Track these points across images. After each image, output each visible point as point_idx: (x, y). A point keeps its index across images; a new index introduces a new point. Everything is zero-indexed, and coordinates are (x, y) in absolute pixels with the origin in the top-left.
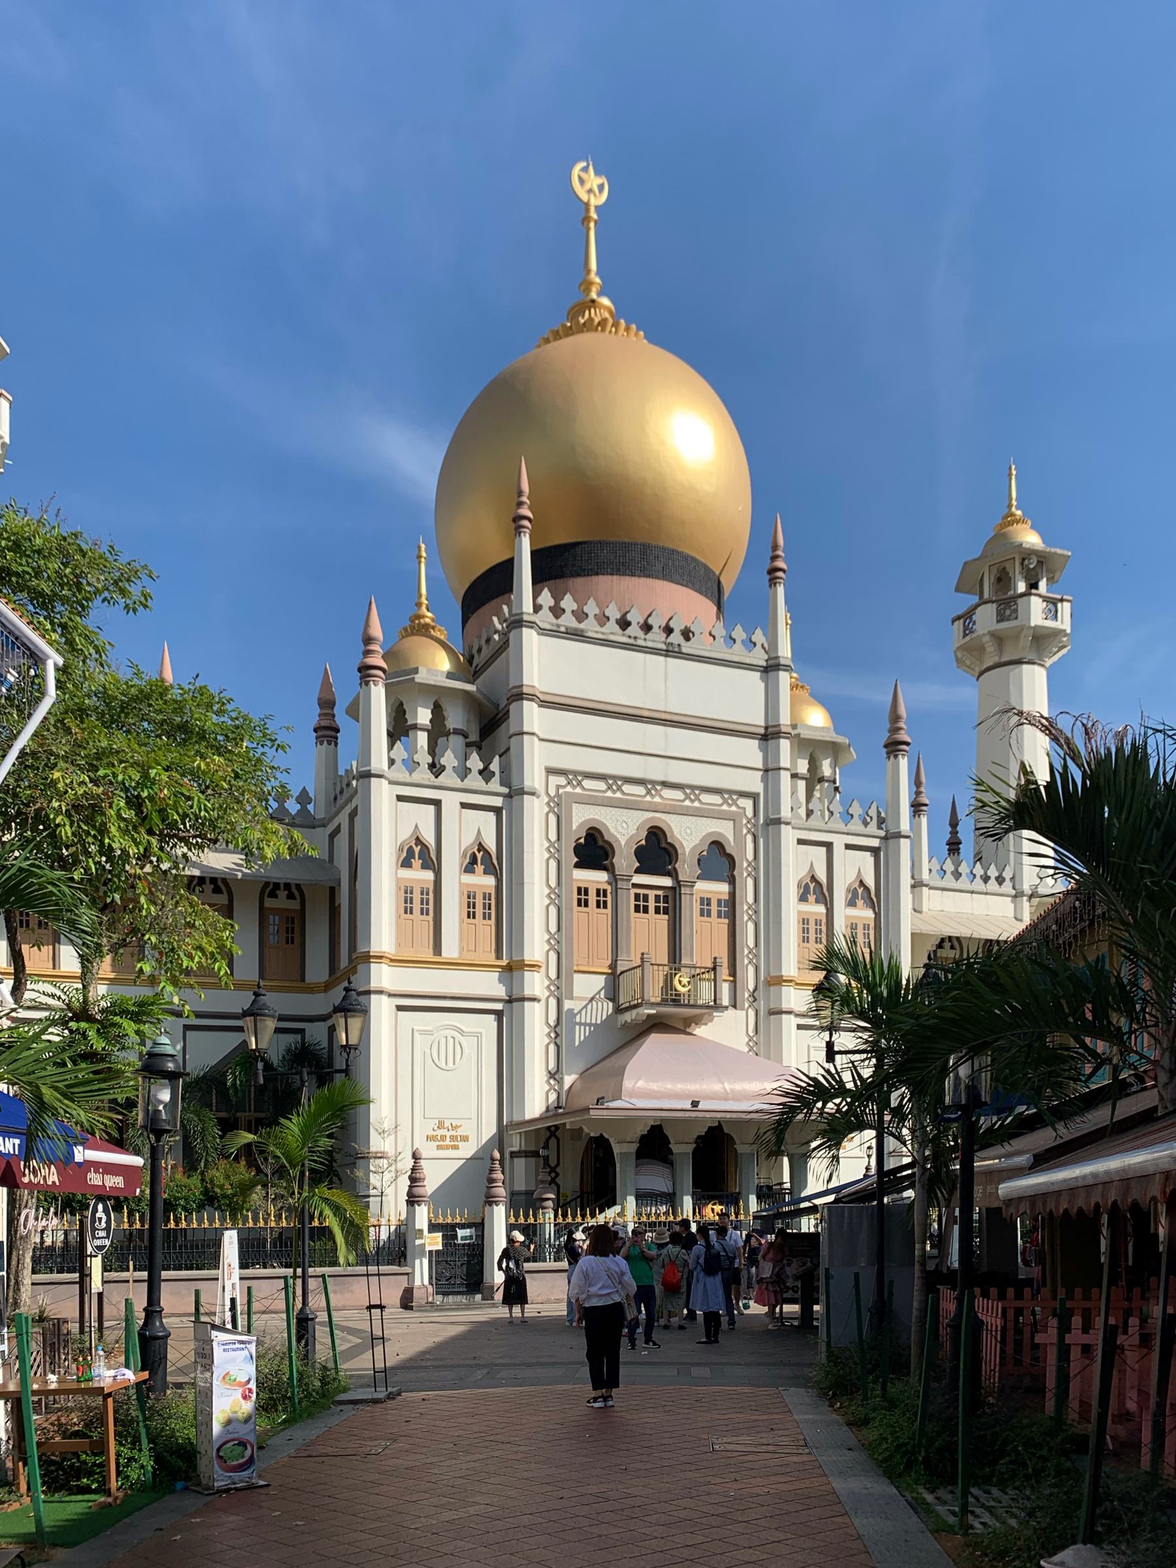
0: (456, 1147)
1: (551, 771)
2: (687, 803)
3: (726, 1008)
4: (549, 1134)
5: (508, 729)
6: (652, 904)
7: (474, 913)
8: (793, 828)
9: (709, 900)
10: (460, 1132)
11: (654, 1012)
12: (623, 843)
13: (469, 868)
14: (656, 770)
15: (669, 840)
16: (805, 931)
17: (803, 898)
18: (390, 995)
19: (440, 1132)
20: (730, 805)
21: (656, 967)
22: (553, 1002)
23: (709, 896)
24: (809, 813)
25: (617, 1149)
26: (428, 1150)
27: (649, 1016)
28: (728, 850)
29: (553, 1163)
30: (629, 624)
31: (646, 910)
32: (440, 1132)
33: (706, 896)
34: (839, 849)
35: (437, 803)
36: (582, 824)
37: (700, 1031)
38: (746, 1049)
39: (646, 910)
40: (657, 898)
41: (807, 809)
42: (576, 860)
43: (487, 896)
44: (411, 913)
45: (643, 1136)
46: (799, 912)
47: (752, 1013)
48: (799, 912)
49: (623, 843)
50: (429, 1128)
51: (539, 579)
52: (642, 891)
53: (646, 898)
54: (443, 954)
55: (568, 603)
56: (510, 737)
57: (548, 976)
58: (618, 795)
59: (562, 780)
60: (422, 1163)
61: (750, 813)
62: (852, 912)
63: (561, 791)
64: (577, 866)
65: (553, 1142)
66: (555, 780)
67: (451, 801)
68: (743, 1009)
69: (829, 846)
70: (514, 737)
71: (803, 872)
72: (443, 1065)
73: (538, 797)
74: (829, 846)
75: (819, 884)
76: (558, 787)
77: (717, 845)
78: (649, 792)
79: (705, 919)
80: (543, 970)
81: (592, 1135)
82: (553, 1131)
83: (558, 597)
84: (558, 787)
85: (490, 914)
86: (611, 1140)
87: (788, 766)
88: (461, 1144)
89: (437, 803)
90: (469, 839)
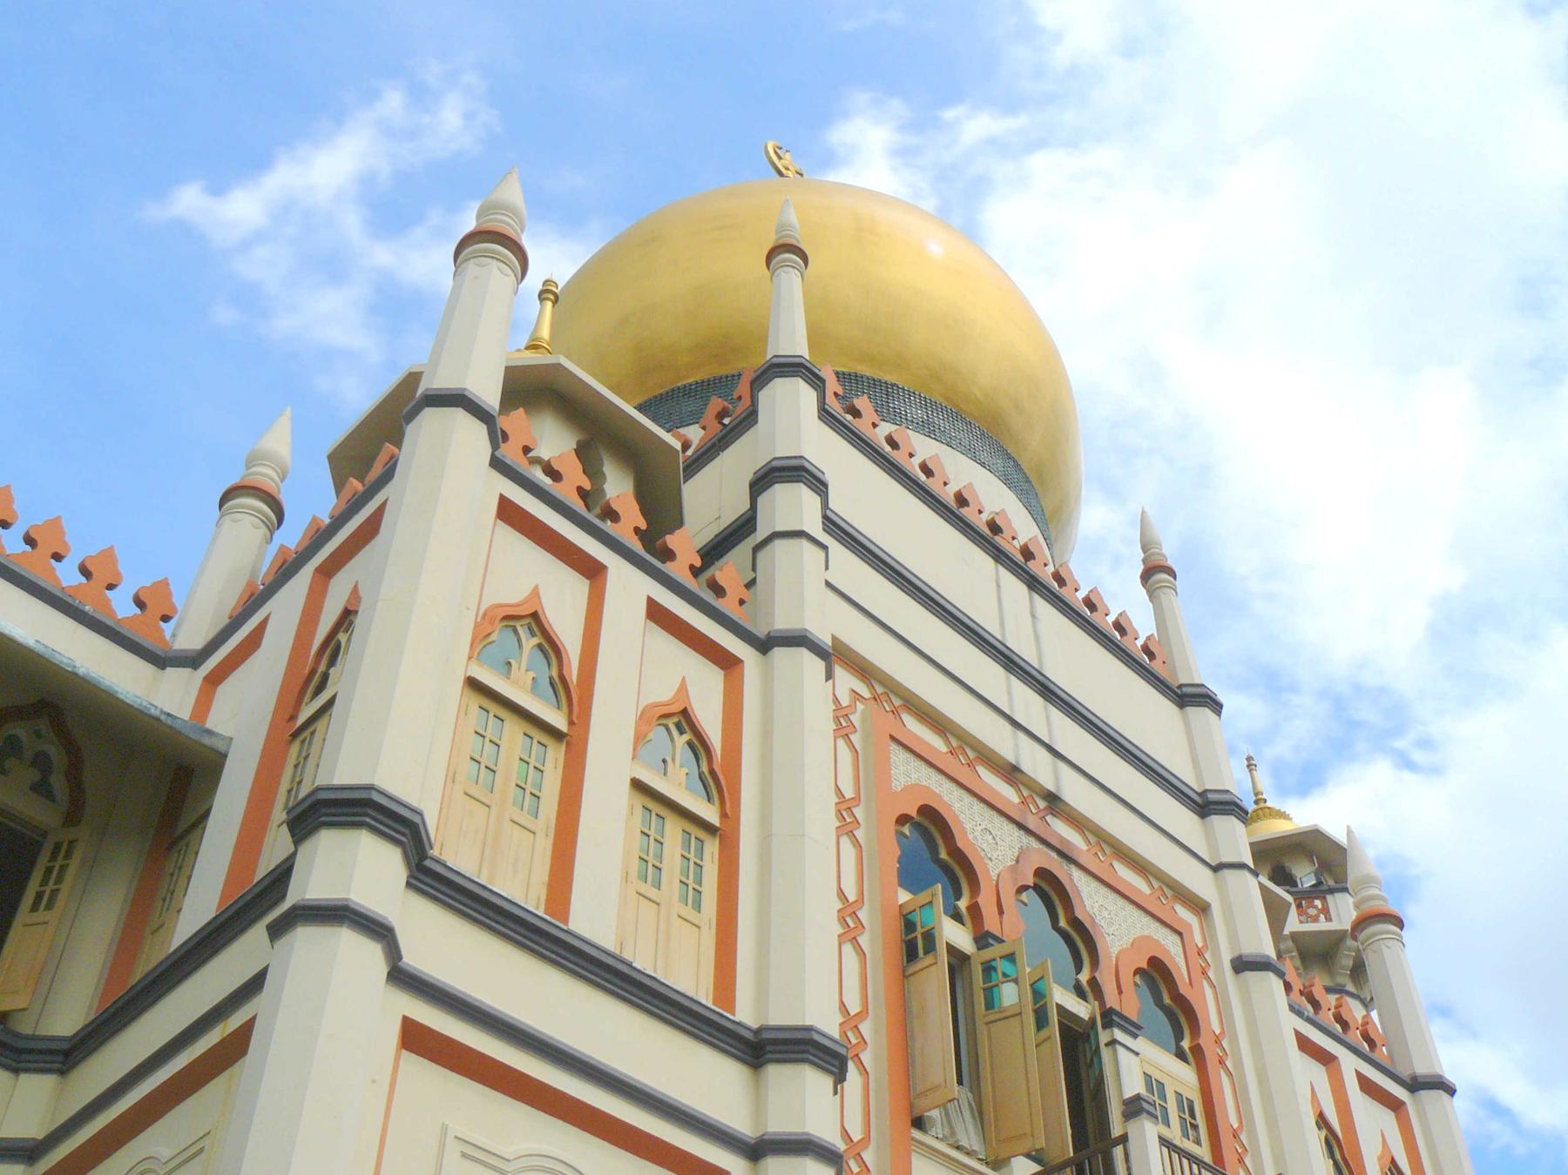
12: (994, 875)
15: (1079, 914)
33: (1156, 1075)
36: (905, 789)
42: (898, 865)
49: (994, 875)
56: (757, 549)
63: (860, 706)
66: (846, 681)
77: (1156, 973)
78: (1024, 802)
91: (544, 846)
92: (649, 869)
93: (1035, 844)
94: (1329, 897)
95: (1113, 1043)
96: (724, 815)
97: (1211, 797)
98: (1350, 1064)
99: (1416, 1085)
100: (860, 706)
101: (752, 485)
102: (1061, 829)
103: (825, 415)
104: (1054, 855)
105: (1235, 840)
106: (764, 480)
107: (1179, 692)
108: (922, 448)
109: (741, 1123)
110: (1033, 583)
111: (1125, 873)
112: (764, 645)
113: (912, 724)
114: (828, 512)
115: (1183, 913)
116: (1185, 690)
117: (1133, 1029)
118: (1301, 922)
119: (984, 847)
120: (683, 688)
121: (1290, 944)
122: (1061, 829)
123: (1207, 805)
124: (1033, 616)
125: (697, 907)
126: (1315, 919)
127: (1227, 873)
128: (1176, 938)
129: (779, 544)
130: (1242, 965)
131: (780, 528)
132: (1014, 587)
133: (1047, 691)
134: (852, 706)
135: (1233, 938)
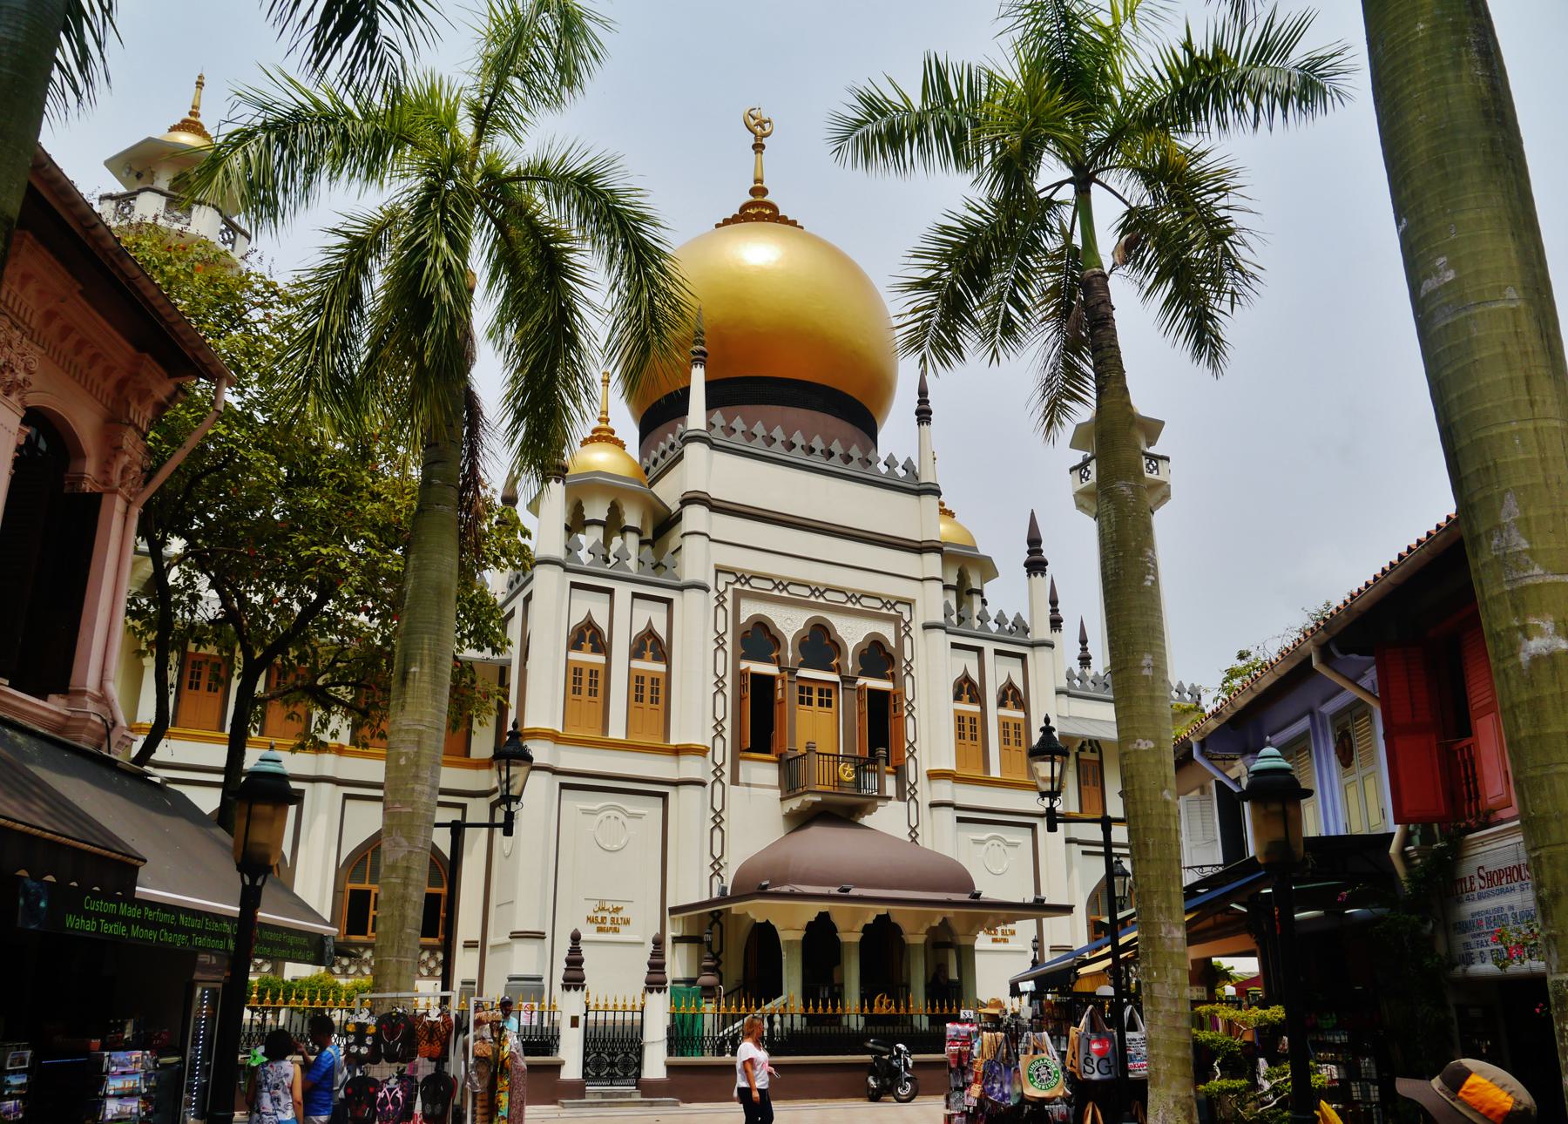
0: (616, 931)
3: (890, 798)
4: (711, 920)
5: (680, 528)
6: (815, 697)
8: (947, 633)
10: (621, 914)
11: (818, 799)
18: (556, 772)
19: (600, 915)
21: (821, 757)
22: (718, 787)
24: (961, 619)
25: (784, 936)
26: (588, 933)
27: (814, 803)
29: (716, 949)
30: (794, 446)
31: (810, 702)
32: (600, 915)
35: (610, 591)
37: (866, 820)
38: (910, 840)
39: (810, 702)
40: (821, 692)
41: (959, 616)
43: (655, 681)
45: (810, 923)
46: (955, 710)
47: (912, 804)
48: (955, 710)
50: (589, 909)
51: (712, 404)
52: (806, 684)
53: (810, 691)
54: (610, 736)
55: (738, 424)
56: (683, 536)
57: (714, 762)
58: (785, 594)
59: (732, 578)
60: (582, 946)
62: (1003, 712)
63: (730, 588)
64: (745, 657)
65: (716, 926)
66: (723, 578)
67: (623, 591)
68: (905, 801)
69: (979, 650)
70: (687, 538)
71: (959, 673)
72: (607, 846)
73: (706, 589)
74: (979, 650)
75: (972, 684)
80: (709, 754)
81: (758, 921)
82: (716, 917)
83: (729, 419)
85: (657, 698)
86: (778, 927)
87: (940, 576)
88: (622, 928)
89: (610, 591)
90: (639, 627)
91: (600, 706)
96: (667, 667)
97: (924, 544)
98: (989, 648)
99: (1033, 645)
100: (730, 588)
105: (932, 564)
107: (916, 487)
109: (675, 777)
112: (681, 589)
114: (714, 503)
115: (899, 607)
116: (922, 487)
119: (786, 626)
120: (650, 621)
123: (920, 548)
125: (657, 703)
127: (926, 583)
129: (687, 538)
130: (926, 627)
131: (688, 530)
134: (726, 590)
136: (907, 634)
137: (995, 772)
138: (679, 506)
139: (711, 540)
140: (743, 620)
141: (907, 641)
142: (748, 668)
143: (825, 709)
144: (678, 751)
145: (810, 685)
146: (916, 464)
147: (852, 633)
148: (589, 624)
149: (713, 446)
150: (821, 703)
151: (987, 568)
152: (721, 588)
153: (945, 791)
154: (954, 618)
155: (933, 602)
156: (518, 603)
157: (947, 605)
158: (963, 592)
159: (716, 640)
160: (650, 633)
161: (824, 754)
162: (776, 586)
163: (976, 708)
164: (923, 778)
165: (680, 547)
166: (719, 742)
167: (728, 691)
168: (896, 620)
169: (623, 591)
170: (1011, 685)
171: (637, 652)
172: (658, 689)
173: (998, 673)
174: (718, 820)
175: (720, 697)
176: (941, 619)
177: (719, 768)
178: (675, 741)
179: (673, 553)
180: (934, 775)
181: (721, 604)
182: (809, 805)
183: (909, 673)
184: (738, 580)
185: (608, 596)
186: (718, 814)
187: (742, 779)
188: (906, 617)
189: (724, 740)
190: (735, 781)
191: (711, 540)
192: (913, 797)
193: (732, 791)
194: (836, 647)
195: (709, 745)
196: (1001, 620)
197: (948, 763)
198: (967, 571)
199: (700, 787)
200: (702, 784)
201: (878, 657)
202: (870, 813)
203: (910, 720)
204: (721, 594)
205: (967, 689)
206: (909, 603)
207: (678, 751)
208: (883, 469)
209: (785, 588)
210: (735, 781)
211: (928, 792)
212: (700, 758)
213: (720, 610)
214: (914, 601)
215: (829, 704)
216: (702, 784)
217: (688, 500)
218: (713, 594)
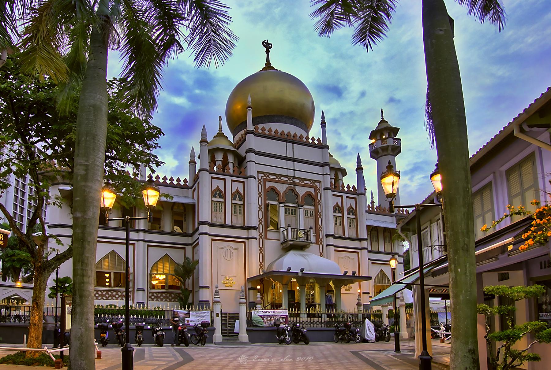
1: (259, 172)
2: (300, 183)
7: (236, 212)
9: (308, 211)
11: (292, 243)
13: (233, 198)
14: (291, 173)
15: (295, 193)
16: (336, 221)
17: (335, 212)
20: (313, 184)
22: (261, 240)
23: (307, 210)
28: (313, 197)
31: (289, 214)
34: (344, 198)
35: (224, 179)
40: (292, 210)
44: (216, 211)
49: (281, 193)
53: (289, 209)
58: (280, 180)
59: (263, 175)
61: (319, 187)
62: (349, 216)
66: (260, 175)
69: (341, 196)
73: (255, 178)
74: (341, 196)
76: (261, 177)
77: (309, 194)
78: (289, 180)
79: (307, 217)
80: (258, 229)
84: (261, 177)
87: (329, 173)
89: (224, 179)
90: (234, 190)
92: (235, 213)
93: (289, 185)
94: (387, 139)
95: (299, 209)
97: (324, 164)
98: (344, 195)
100: (262, 178)
101: (246, 152)
102: (296, 180)
103: (256, 135)
104: (293, 186)
105: (327, 169)
106: (247, 152)
108: (275, 127)
110: (293, 143)
111: (306, 182)
112: (247, 178)
113: (270, 176)
115: (316, 184)
116: (323, 146)
117: (302, 206)
118: (382, 144)
121: (380, 149)
122: (296, 180)
124: (293, 148)
126: (384, 144)
128: (313, 189)
129: (248, 162)
130: (325, 189)
132: (290, 145)
133: (294, 160)
135: (324, 185)
136: (319, 192)
137: (346, 235)
138: (245, 154)
139: (256, 163)
140: (267, 187)
141: (319, 194)
142: (269, 203)
143: (293, 215)
144: (248, 228)
145: (289, 208)
146: (321, 139)
147: (301, 191)
148: (218, 189)
149: (255, 135)
150: (292, 214)
151: (344, 172)
152: (260, 178)
153: (332, 241)
154: (334, 187)
155: (328, 181)
156: (196, 185)
157: (331, 182)
158: (337, 180)
159: (259, 194)
160: (237, 191)
161: (293, 228)
162: (277, 178)
163: (340, 215)
164: (325, 237)
165: (246, 167)
166: (261, 226)
167: (263, 210)
168: (315, 187)
169: (229, 179)
170: (351, 207)
171: (234, 197)
172: (241, 209)
173: (348, 203)
174: (261, 250)
175: (260, 212)
176: (329, 186)
177: (261, 234)
178: (246, 225)
179: (245, 169)
180: (328, 236)
181: (260, 183)
182: (289, 245)
183: (319, 204)
184: (265, 176)
185: (224, 181)
186: (261, 248)
187: (268, 238)
188: (319, 187)
189: (262, 225)
190: (266, 238)
191: (256, 163)
192: (321, 243)
193: (265, 240)
194: (297, 195)
195: (258, 227)
196: (348, 187)
197: (332, 232)
198: (337, 173)
199: (255, 240)
200: (256, 238)
201: (311, 199)
202: (308, 248)
203: (320, 219)
204: (260, 180)
205: (338, 209)
206: (320, 182)
207: (248, 228)
208: (311, 141)
209: (280, 178)
210: (266, 238)
211: (325, 241)
212: (255, 230)
213: (260, 185)
214: (321, 181)
215: (295, 214)
216: (256, 238)
217: (249, 151)
218: (257, 180)
